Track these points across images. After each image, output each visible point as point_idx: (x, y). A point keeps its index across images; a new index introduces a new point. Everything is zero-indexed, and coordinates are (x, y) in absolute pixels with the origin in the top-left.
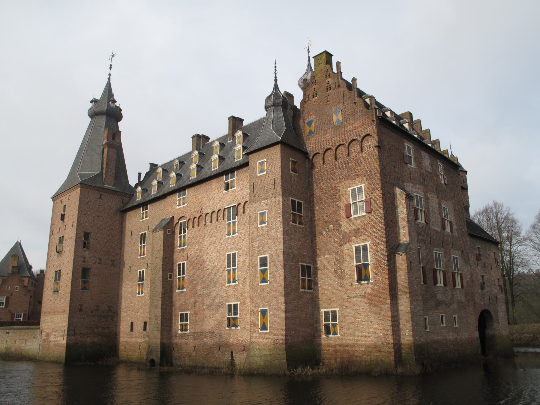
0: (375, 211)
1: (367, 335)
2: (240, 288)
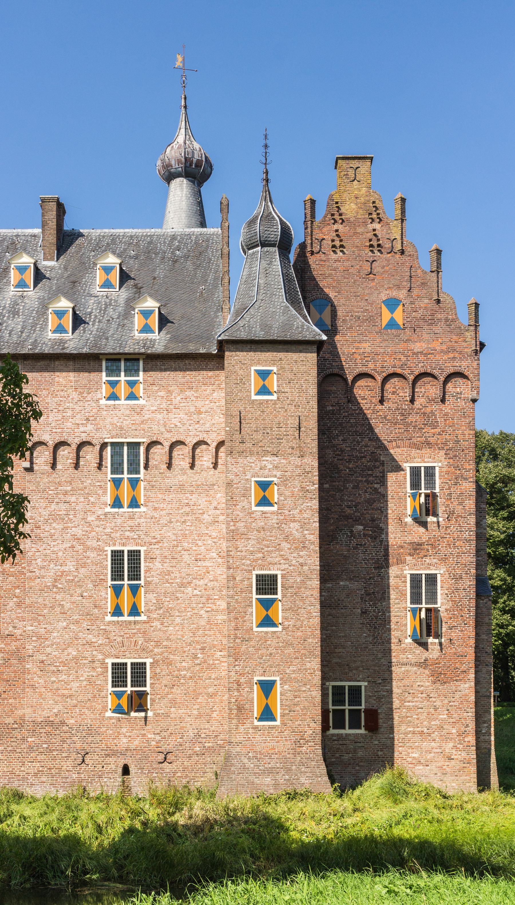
0: (458, 516)
1: (425, 730)
2: (152, 628)
